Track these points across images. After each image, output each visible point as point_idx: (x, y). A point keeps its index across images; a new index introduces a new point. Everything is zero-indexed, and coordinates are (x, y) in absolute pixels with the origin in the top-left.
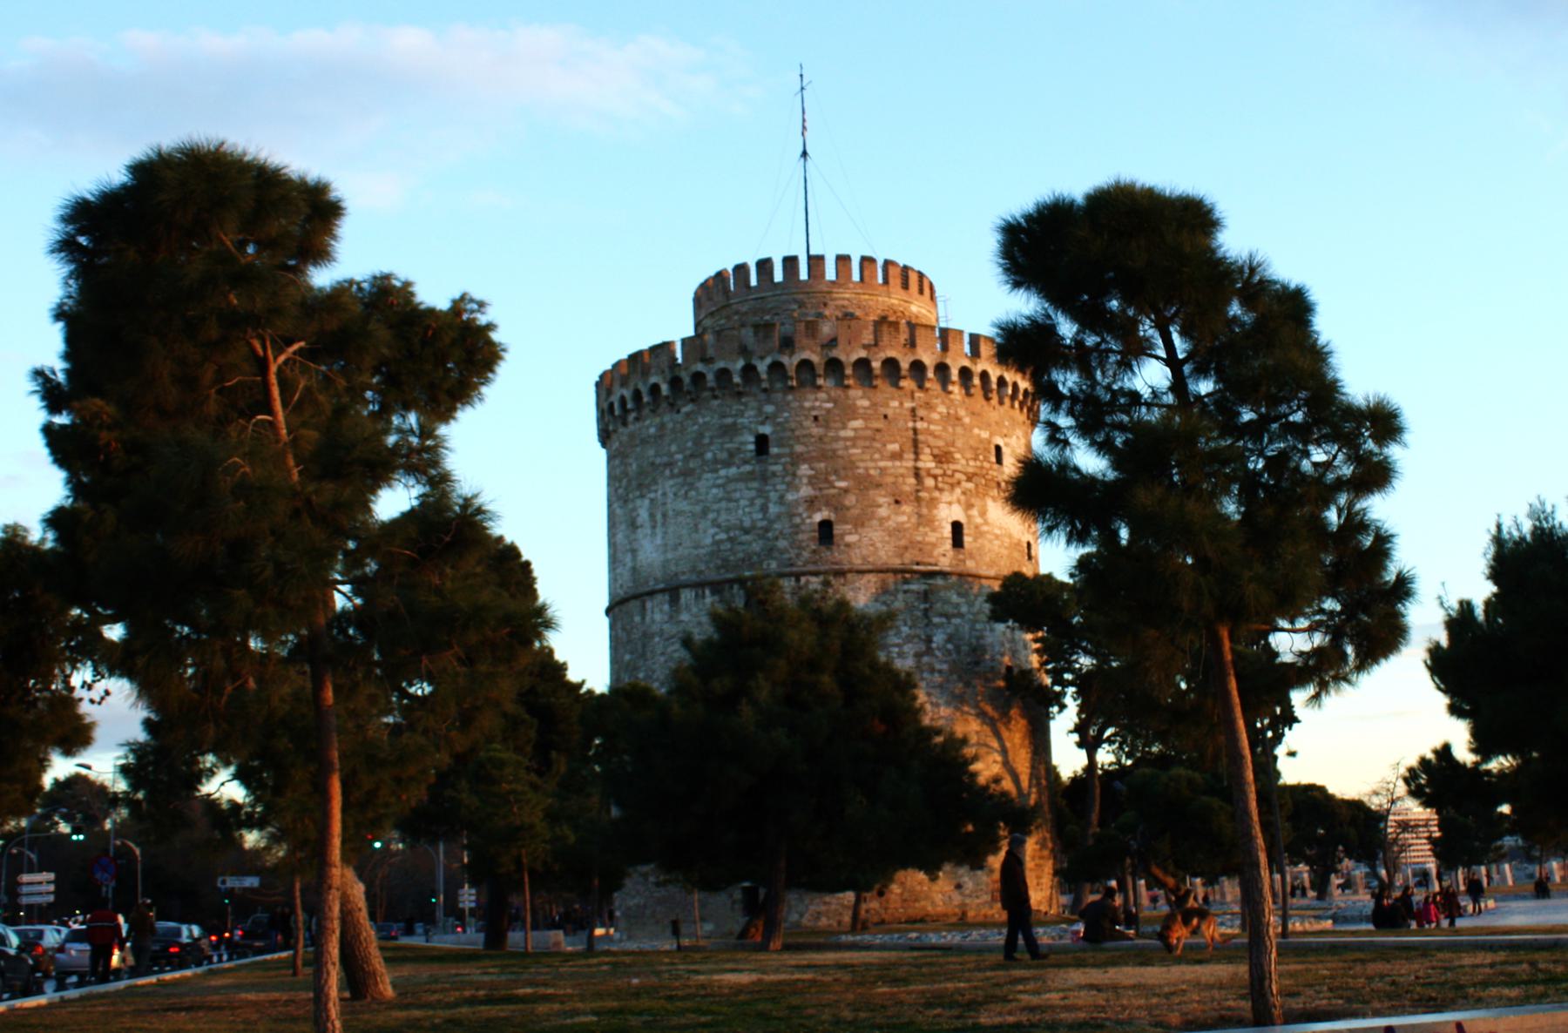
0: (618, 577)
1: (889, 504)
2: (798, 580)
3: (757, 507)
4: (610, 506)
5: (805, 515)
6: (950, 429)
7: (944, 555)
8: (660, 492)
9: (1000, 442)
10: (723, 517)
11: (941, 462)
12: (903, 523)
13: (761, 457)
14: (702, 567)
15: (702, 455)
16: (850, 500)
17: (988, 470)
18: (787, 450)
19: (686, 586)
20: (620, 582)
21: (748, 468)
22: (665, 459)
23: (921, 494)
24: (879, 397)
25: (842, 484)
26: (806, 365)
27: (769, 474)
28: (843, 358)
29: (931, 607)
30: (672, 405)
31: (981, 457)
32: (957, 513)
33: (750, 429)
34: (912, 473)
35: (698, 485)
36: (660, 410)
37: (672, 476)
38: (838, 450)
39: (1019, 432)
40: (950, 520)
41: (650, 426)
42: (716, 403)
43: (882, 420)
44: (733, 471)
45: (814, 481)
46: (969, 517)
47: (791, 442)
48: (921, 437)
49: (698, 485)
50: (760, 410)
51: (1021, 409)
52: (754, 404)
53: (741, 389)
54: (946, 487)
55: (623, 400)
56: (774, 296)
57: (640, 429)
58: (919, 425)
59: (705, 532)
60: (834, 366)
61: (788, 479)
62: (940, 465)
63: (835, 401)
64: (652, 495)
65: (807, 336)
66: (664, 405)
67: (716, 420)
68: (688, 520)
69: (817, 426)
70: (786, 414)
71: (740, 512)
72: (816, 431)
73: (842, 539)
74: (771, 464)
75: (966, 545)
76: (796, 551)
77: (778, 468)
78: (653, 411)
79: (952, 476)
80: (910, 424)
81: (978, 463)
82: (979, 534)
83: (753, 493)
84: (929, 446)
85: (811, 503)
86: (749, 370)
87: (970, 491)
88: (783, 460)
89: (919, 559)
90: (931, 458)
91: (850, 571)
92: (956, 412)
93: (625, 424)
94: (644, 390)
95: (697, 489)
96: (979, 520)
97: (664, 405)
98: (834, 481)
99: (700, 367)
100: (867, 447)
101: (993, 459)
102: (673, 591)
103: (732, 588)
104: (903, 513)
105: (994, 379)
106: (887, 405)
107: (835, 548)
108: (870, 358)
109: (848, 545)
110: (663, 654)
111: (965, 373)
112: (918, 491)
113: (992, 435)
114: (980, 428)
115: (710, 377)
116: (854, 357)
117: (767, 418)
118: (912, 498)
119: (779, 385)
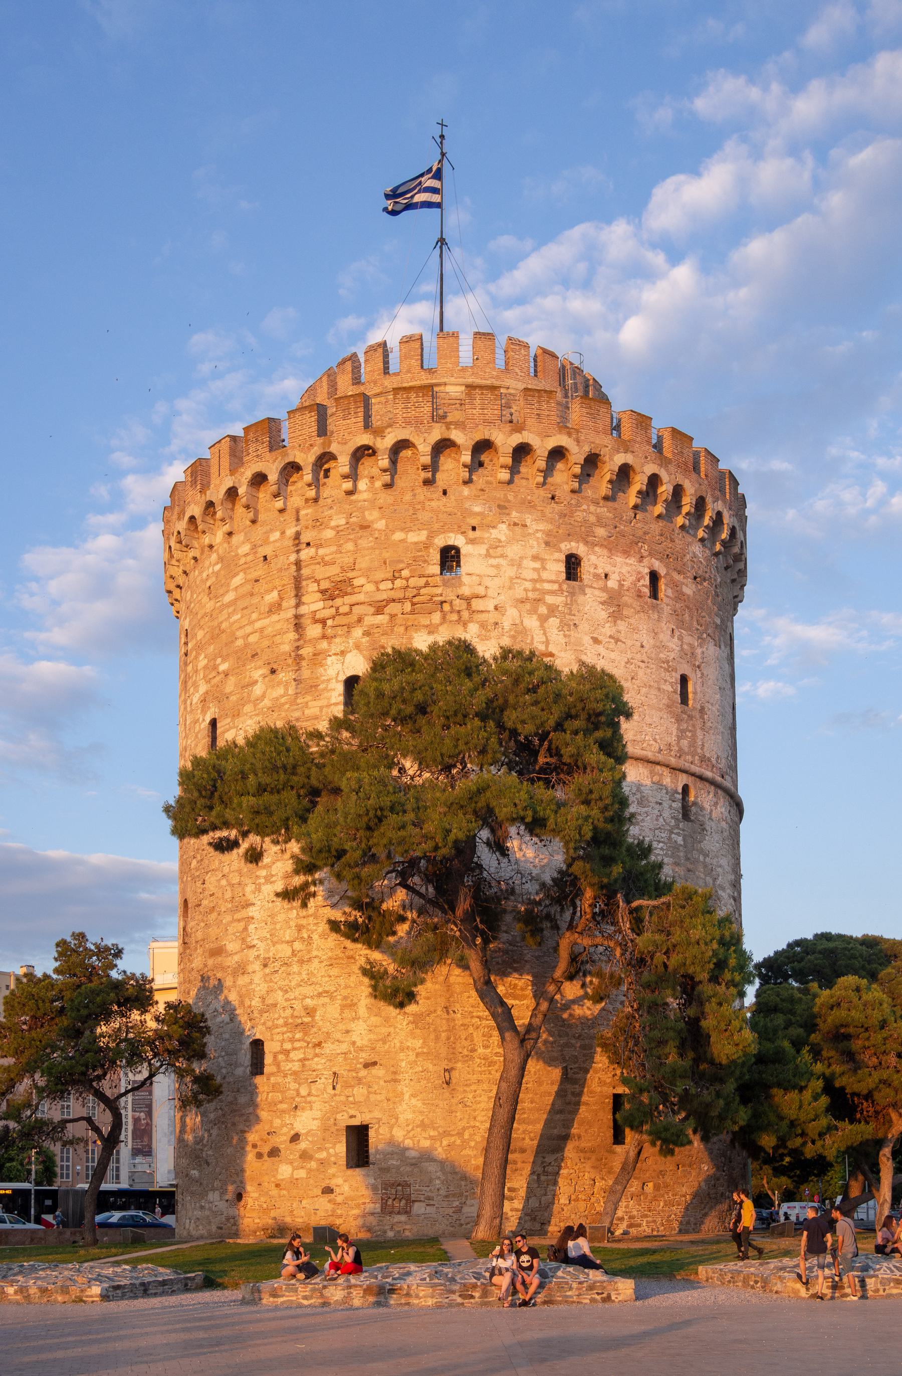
6: (350, 546)
12: (277, 699)
31: (405, 573)
34: (291, 627)
40: (342, 677)
58: (306, 554)
62: (330, 603)
90: (320, 594)
101: (436, 569)
104: (279, 683)
112: (298, 648)
118: (290, 661)
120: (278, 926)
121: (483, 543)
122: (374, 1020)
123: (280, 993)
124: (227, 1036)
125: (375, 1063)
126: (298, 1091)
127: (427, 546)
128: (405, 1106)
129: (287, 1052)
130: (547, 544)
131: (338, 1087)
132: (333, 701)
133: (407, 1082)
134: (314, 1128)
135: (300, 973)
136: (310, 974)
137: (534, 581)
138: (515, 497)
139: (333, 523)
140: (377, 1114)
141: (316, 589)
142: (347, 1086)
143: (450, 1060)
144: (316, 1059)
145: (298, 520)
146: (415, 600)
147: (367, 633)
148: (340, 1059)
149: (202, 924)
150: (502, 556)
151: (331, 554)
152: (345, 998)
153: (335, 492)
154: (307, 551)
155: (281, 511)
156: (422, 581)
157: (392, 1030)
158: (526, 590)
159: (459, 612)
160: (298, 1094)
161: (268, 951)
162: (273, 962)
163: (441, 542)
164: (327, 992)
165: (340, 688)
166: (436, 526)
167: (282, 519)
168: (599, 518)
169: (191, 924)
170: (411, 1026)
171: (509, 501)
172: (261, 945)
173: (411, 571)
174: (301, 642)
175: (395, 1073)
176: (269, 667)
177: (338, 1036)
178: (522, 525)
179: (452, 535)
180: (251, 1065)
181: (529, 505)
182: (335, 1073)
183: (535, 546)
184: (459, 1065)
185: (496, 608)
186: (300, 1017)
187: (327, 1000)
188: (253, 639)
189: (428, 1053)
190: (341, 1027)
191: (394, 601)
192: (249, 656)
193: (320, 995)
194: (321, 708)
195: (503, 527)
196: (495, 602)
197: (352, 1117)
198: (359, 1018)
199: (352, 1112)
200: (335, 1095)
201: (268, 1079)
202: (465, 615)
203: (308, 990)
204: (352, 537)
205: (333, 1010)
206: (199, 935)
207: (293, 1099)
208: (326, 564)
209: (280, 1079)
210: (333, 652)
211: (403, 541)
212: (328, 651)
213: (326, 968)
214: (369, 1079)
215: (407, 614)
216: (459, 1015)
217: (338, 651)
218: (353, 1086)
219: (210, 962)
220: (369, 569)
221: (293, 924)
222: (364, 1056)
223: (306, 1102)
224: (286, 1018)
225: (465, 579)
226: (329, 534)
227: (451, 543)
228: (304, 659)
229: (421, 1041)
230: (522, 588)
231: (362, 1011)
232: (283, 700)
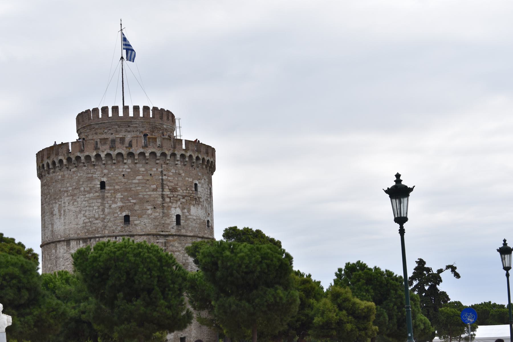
0: (46, 234)
1: (152, 209)
2: (116, 238)
3: (100, 210)
4: (42, 204)
5: (119, 213)
6: (176, 179)
7: (173, 228)
8: (63, 202)
9: (197, 183)
10: (87, 214)
11: (172, 192)
12: (157, 216)
13: (102, 190)
14: (79, 232)
15: (79, 188)
16: (137, 207)
18: (112, 188)
19: (73, 240)
20: (47, 236)
21: (97, 194)
22: (65, 189)
23: (164, 204)
24: (148, 167)
25: (134, 201)
26: (120, 154)
27: (106, 197)
28: (134, 152)
29: (167, 248)
30: (68, 168)
31: (189, 189)
32: (179, 211)
33: (98, 179)
34: (161, 197)
35: (78, 200)
36: (63, 170)
37: (68, 196)
38: (132, 188)
39: (205, 177)
41: (59, 175)
42: (85, 168)
43: (149, 176)
44: (91, 195)
45: (122, 200)
46: (183, 213)
47: (114, 185)
48: (165, 182)
49: (78, 200)
50: (102, 171)
51: (206, 167)
52: (100, 169)
53: (94, 163)
54: (175, 201)
55: (48, 165)
56: (108, 122)
57: (55, 176)
58: (164, 177)
59: (80, 218)
60: (131, 155)
61: (113, 199)
62: (172, 193)
63: (131, 169)
64: (60, 203)
65: (121, 144)
66: (65, 167)
67: (85, 175)
68: (74, 214)
69: (124, 178)
70: (112, 174)
71: (94, 211)
72: (123, 180)
73: (134, 222)
74: (106, 193)
75: (182, 224)
76: (116, 227)
77: (109, 195)
78: (60, 170)
79: (177, 196)
80: (161, 177)
81: (187, 191)
82: (187, 219)
83: (99, 204)
84: (167, 186)
85: (121, 209)
86: (98, 156)
88: (111, 191)
89: (163, 230)
90: (168, 190)
91: (136, 235)
93: (49, 173)
94: (57, 162)
95: (78, 202)
96: (187, 214)
97: (65, 167)
98: (130, 200)
99: (79, 154)
100: (144, 187)
101: (194, 189)
102: (68, 241)
103: (90, 241)
104: (157, 212)
105: (194, 158)
106: (151, 170)
107: (130, 225)
108: (145, 152)
109: (135, 225)
110: (63, 265)
111: (183, 156)
112: (163, 203)
113: (193, 180)
115: (83, 158)
116: (138, 152)
117: (105, 175)
118: (161, 206)
119: (109, 162)
127: (192, 182)
128: (193, 333)
132: (173, 220)
134: (172, 338)
139: (172, 171)
140: (187, 335)
145: (162, 167)
146: (191, 196)
150: (203, 187)
151: (172, 179)
155: (157, 163)
165: (175, 217)
167: (157, 165)
174: (164, 202)
185: (203, 201)
191: (186, 196)
194: (170, 222)
197: (182, 335)
199: (182, 334)
202: (199, 202)
204: (177, 176)
208: (170, 182)
212: (172, 206)
217: (174, 207)
225: (199, 193)
227: (196, 183)
232: (158, 217)
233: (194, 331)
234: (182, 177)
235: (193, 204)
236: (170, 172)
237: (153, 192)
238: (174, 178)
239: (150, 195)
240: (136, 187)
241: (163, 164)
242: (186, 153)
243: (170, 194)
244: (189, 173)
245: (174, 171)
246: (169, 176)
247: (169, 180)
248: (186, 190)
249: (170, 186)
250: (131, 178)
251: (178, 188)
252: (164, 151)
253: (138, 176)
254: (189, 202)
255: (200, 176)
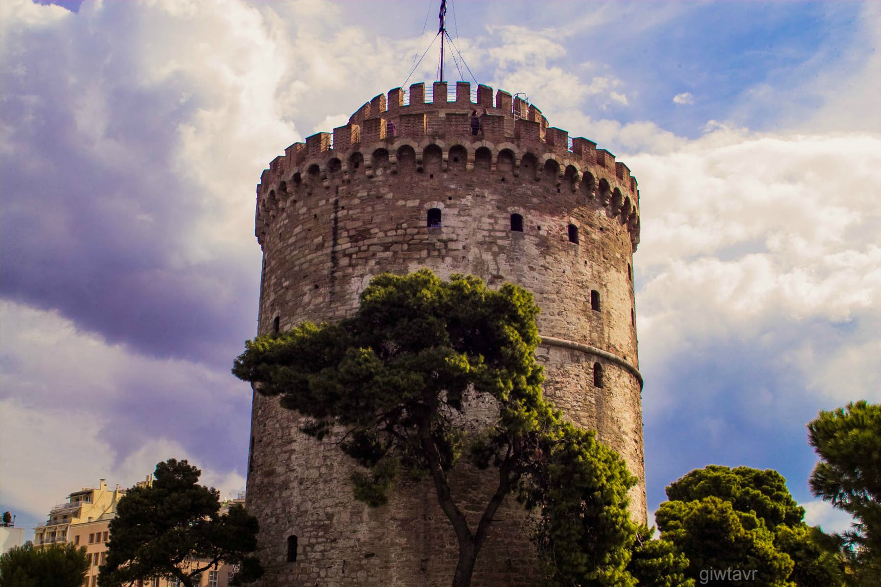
6: (369, 209)
9: (440, 206)
11: (357, 241)
12: (318, 304)
17: (413, 235)
23: (336, 274)
31: (404, 226)
34: (329, 259)
54: (360, 262)
58: (340, 214)
62: (356, 244)
79: (368, 249)
87: (386, 259)
90: (348, 239)
92: (378, 192)
100: (302, 247)
101: (424, 223)
104: (320, 295)
106: (317, 206)
112: (333, 272)
113: (423, 202)
114: (406, 199)
120: (311, 457)
121: (457, 207)
122: (373, 524)
123: (310, 503)
124: (273, 533)
125: (372, 555)
126: (318, 573)
127: (419, 208)
129: (312, 546)
130: (498, 207)
131: (346, 571)
132: (355, 306)
133: (395, 569)
135: (324, 490)
136: (331, 490)
137: (490, 231)
138: (477, 179)
139: (359, 195)
141: (346, 235)
142: (353, 571)
143: (426, 553)
144: (332, 551)
147: (377, 263)
148: (349, 551)
149: (262, 454)
150: (468, 215)
152: (354, 508)
153: (361, 177)
154: (342, 212)
155: (327, 188)
156: (416, 231)
157: (385, 530)
158: (484, 236)
159: (439, 250)
160: (319, 576)
161: (303, 473)
162: (307, 481)
163: (428, 206)
164: (341, 503)
166: (426, 197)
167: (327, 192)
168: (533, 191)
169: (256, 454)
170: (400, 528)
171: (474, 182)
172: (299, 469)
173: (408, 225)
174: (336, 268)
175: (387, 562)
176: (314, 284)
177: (348, 534)
178: (482, 196)
179: (435, 202)
180: (288, 554)
181: (487, 185)
182: (344, 561)
183: (490, 209)
184: (432, 557)
185: (464, 247)
186: (323, 521)
187: (341, 509)
188: (305, 266)
189: (410, 548)
190: (350, 528)
191: (396, 243)
192: (302, 276)
193: (337, 505)
194: (346, 311)
195: (470, 197)
196: (464, 244)
198: (363, 522)
200: (344, 577)
201: (299, 564)
202: (444, 252)
203: (328, 502)
205: (345, 516)
206: (260, 461)
207: (315, 579)
209: (307, 565)
210: (356, 275)
211: (405, 206)
213: (342, 486)
214: (368, 566)
215: (404, 251)
216: (433, 521)
218: (357, 571)
219: (266, 480)
220: (381, 223)
221: (321, 455)
222: (365, 549)
223: (324, 582)
224: (314, 521)
225: (444, 230)
226: (356, 201)
227: (434, 207)
228: (337, 279)
229: (406, 539)
230: (482, 235)
231: (365, 516)
232: (322, 306)
233: (399, 583)
234: (387, 202)
235: (417, 259)
236: (356, 197)
237: (315, 252)
238: (364, 209)
239: (311, 260)
240: (291, 251)
241: (341, 186)
242: (390, 145)
243: (351, 247)
244: (409, 188)
245: (365, 194)
246: (351, 208)
247: (352, 216)
248: (396, 230)
249: (352, 229)
250: (287, 236)
251: (373, 228)
252: (334, 156)
253: (296, 227)
254: (403, 254)
255: (453, 189)
